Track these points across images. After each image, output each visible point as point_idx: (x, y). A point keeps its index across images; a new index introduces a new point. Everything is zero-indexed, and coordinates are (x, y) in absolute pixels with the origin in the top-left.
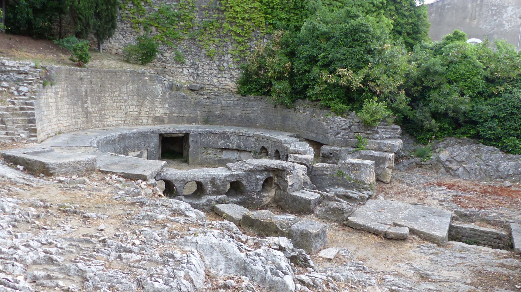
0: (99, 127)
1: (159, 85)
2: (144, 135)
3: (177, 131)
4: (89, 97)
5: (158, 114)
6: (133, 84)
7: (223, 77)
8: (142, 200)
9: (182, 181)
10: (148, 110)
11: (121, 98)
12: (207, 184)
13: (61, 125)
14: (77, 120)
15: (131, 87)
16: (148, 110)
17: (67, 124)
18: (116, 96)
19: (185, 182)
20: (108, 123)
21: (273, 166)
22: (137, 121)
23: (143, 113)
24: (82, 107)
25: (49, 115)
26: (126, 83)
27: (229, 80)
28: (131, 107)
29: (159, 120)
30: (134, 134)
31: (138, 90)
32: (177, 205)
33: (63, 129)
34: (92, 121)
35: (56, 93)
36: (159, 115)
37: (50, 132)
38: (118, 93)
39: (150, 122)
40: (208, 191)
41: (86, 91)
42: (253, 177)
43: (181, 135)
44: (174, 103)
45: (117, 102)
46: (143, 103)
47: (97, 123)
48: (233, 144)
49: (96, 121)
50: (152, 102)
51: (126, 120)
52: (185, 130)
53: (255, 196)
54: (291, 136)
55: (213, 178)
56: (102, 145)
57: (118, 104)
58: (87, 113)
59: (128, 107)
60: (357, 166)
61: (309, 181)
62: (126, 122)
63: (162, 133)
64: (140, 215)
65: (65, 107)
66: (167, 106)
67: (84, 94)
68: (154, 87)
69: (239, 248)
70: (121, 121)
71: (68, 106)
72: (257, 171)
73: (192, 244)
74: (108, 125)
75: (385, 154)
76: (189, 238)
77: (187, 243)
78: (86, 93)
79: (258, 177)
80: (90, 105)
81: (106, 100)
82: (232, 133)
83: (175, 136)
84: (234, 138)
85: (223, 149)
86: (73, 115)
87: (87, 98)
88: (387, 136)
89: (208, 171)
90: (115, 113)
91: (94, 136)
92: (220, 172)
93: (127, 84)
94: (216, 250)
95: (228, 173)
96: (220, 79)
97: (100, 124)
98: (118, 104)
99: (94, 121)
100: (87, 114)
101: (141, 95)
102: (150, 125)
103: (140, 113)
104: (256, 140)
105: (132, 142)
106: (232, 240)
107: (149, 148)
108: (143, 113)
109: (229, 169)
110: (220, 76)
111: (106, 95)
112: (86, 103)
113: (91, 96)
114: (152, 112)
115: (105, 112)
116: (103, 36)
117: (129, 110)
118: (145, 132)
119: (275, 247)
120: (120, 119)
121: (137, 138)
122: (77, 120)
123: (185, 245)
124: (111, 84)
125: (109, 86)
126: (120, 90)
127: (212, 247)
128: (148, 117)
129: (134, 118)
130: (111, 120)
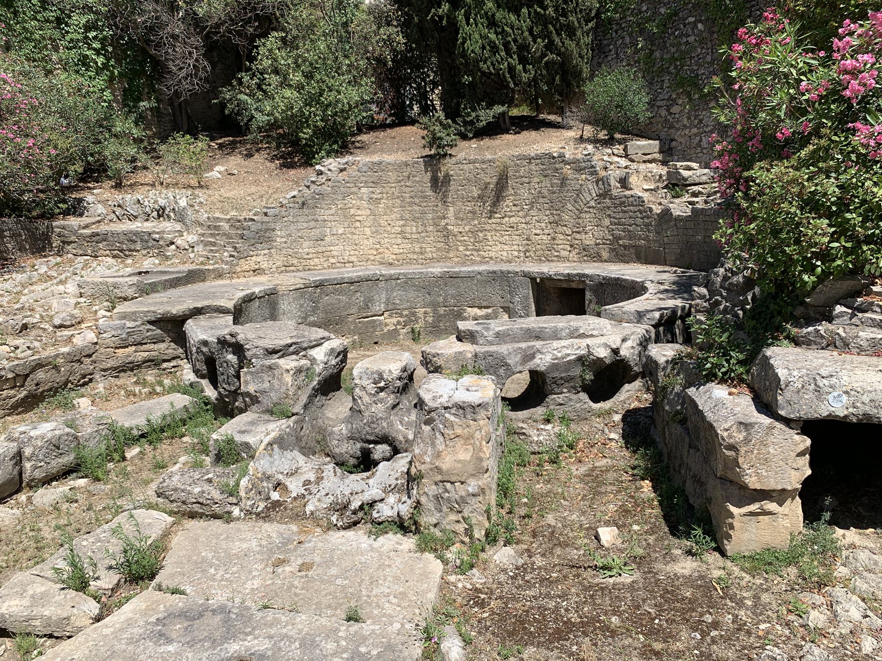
10: (569, 232)
11: (519, 208)
14: (424, 245)
18: (507, 206)
20: (492, 254)
30: (480, 273)
37: (353, 259)
43: (574, 285)
45: (510, 217)
47: (468, 253)
51: (527, 251)
52: (578, 275)
57: (513, 219)
58: (447, 235)
62: (528, 254)
65: (393, 221)
66: (607, 222)
71: (402, 222)
74: (491, 258)
83: (565, 286)
90: (507, 237)
99: (461, 248)
103: (554, 239)
112: (444, 218)
114: (578, 236)
122: (424, 245)
128: (571, 246)
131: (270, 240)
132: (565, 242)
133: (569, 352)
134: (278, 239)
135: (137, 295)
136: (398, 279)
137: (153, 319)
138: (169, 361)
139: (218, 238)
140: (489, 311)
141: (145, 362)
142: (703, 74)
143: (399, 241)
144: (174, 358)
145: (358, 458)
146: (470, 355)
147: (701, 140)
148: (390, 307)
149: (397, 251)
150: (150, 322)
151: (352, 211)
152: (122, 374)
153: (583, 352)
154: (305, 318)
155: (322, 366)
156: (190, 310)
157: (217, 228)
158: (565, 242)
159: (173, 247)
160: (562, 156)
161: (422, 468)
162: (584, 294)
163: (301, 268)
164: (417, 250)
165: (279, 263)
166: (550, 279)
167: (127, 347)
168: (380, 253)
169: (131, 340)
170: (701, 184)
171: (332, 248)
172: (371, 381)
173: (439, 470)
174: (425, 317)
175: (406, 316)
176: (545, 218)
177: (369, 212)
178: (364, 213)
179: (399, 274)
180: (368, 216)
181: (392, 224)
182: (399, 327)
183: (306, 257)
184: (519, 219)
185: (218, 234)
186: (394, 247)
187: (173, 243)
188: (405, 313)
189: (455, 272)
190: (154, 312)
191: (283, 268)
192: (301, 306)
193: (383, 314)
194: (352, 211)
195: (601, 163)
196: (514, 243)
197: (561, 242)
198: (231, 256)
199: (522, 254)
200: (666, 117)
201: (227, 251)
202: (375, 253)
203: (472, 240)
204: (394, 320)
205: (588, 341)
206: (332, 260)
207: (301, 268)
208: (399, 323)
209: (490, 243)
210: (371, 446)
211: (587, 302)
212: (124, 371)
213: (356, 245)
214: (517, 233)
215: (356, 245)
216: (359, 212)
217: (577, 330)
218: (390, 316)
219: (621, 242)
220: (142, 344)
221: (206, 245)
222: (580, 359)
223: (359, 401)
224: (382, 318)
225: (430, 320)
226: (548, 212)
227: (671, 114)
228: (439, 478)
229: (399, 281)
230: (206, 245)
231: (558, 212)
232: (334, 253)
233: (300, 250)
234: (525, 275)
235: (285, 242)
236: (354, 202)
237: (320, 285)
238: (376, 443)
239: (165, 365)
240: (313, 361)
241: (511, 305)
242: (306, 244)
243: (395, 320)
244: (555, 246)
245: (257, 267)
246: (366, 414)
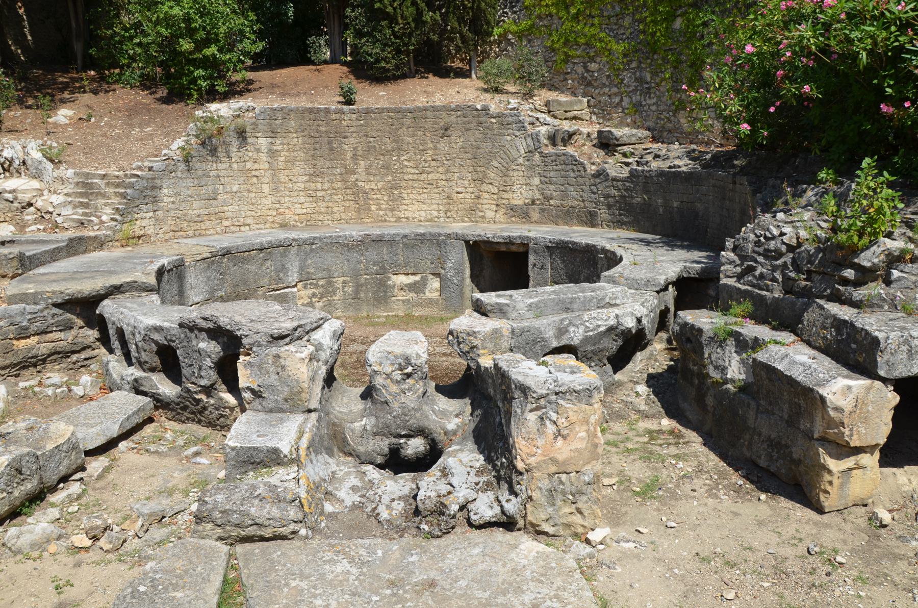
0: (385, 221)
3: (503, 238)
10: (495, 190)
11: (438, 163)
13: (287, 211)
14: (330, 204)
16: (495, 190)
17: (305, 211)
18: (425, 161)
20: (408, 214)
22: (472, 211)
25: (249, 191)
29: (521, 213)
30: (406, 236)
33: (290, 217)
35: (272, 153)
36: (520, 202)
37: (249, 221)
38: (430, 152)
43: (514, 248)
44: (552, 174)
46: (485, 176)
47: (381, 213)
51: (449, 210)
52: (519, 237)
55: (135, 327)
57: (430, 176)
58: (357, 192)
59: (453, 183)
62: (449, 214)
66: (536, 181)
67: (349, 156)
68: (509, 138)
70: (439, 211)
71: (306, 178)
72: (201, 330)
74: (407, 218)
79: (202, 345)
83: (503, 249)
86: (320, 194)
97: (390, 214)
99: (373, 208)
102: (501, 222)
103: (478, 197)
108: (486, 195)
114: (506, 195)
120: (435, 206)
122: (330, 204)
126: (435, 148)
128: (497, 205)
129: (467, 207)
130: (415, 207)
131: (155, 200)
132: (490, 202)
133: (599, 323)
134: (165, 199)
135: (20, 271)
136: (313, 244)
137: (60, 301)
138: (78, 352)
139: (91, 198)
140: (417, 278)
141: (49, 356)
142: (623, 34)
143: (302, 200)
144: (84, 349)
145: (386, 455)
146: (506, 333)
147: (621, 100)
148: (305, 277)
149: (299, 211)
150: (56, 305)
151: (249, 165)
152: (23, 373)
153: (612, 323)
154: (211, 293)
155: (328, 352)
156: (107, 288)
157: (90, 186)
158: (490, 202)
159: (32, 209)
160: (485, 109)
161: (532, 461)
162: (528, 258)
163: (191, 233)
164: (323, 210)
165: (165, 228)
166: (488, 243)
167: (29, 337)
168: (280, 214)
169: (34, 328)
170: (630, 144)
171: (226, 208)
172: (397, 366)
173: (553, 460)
174: (344, 287)
175: (322, 286)
176: (468, 175)
177: (267, 166)
178: (262, 167)
179: (315, 238)
180: (266, 170)
181: (294, 179)
182: (314, 300)
183: (197, 219)
184: (438, 175)
185: (92, 194)
186: (297, 207)
187: (30, 205)
188: (321, 283)
189: (378, 236)
190: (61, 292)
191: (171, 234)
192: (209, 278)
193: (296, 285)
194: (249, 165)
195: (528, 119)
197: (485, 201)
198: (112, 219)
199: (442, 214)
200: (583, 74)
201: (106, 213)
202: (274, 214)
203: (385, 198)
204: (309, 292)
205: (616, 311)
206: (226, 223)
207: (191, 233)
208: (314, 295)
210: (402, 441)
211: (530, 267)
212: (24, 367)
213: (253, 204)
214: (437, 191)
215: (253, 204)
216: (256, 166)
217: (603, 299)
218: (305, 287)
219: (552, 202)
220: (46, 333)
221: (75, 207)
222: (611, 329)
223: (384, 391)
224: (295, 289)
225: (349, 290)
226: (471, 169)
227: (588, 71)
228: (554, 469)
229: (314, 247)
230: (75, 207)
231: (482, 169)
232: (228, 214)
233: (190, 212)
234: (457, 237)
235: (173, 202)
236: (250, 154)
237: (227, 253)
238: (408, 436)
239: (75, 357)
240: (319, 347)
241: (442, 271)
242: (196, 204)
243: (309, 292)
244: (480, 206)
245: (142, 233)
246: (396, 405)
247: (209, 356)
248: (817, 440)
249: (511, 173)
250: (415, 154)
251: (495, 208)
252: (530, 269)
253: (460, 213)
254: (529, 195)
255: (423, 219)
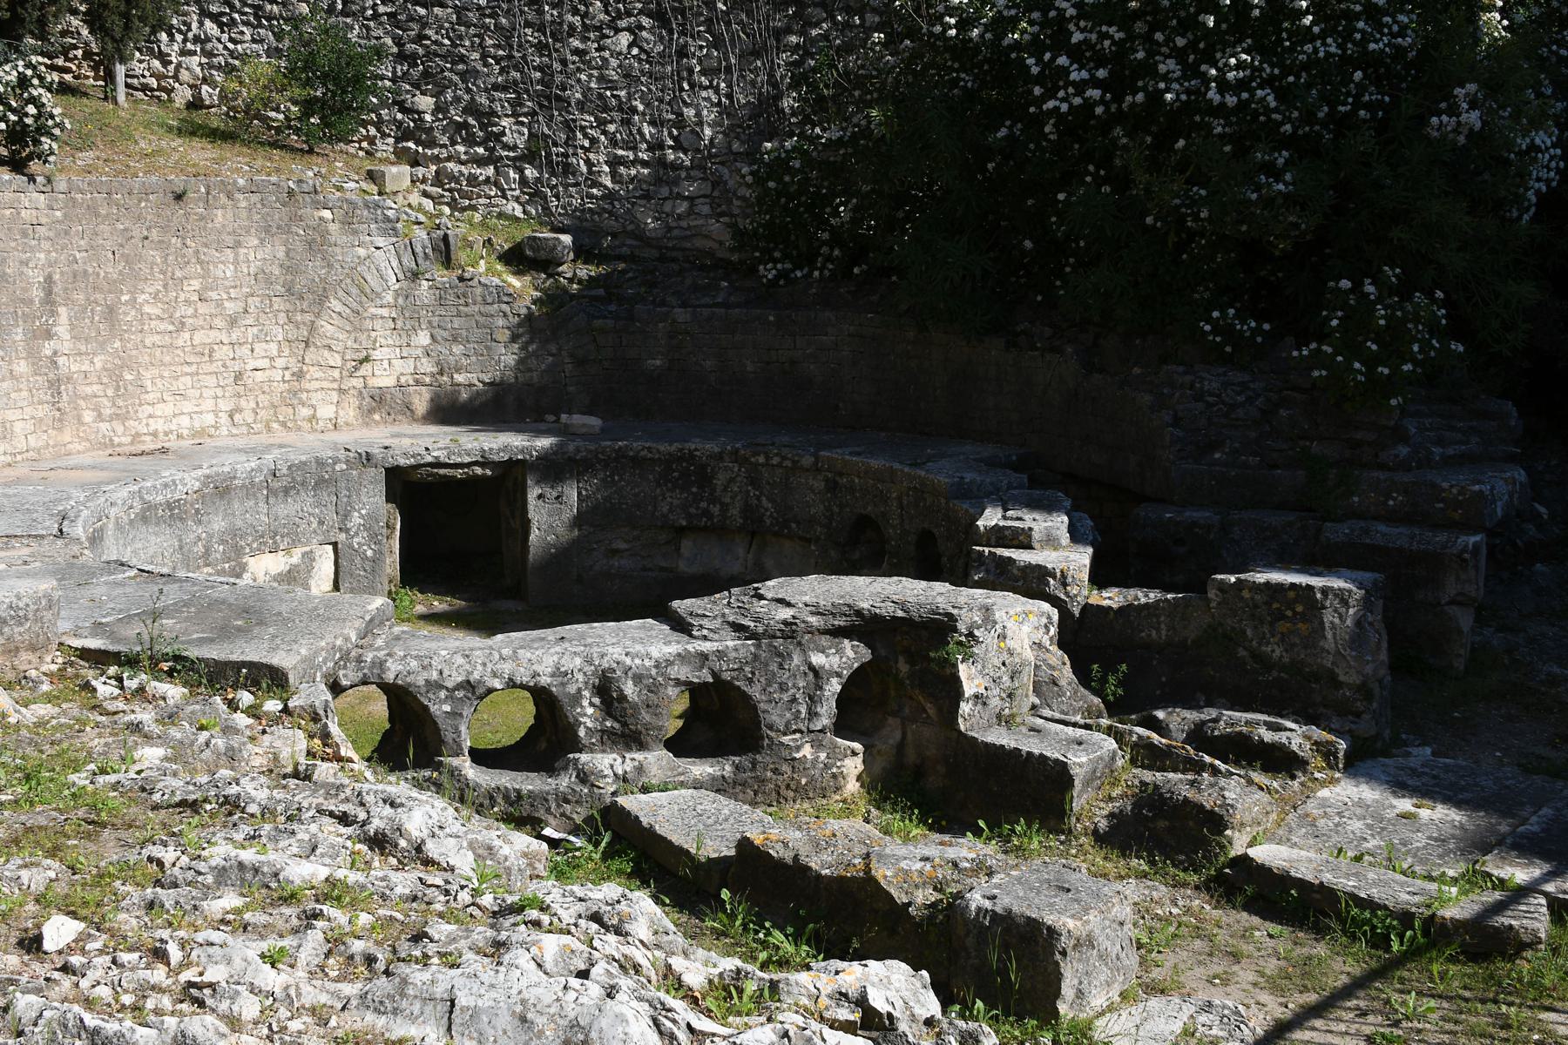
1: (380, 241)
2: (314, 478)
4: (62, 310)
5: (384, 379)
6: (262, 241)
7: (680, 196)
8: (233, 790)
9: (459, 687)
12: (576, 699)
15: (258, 254)
16: (336, 360)
19: (473, 690)
20: (158, 425)
21: (887, 610)
23: (314, 372)
24: (33, 355)
26: (229, 240)
27: (706, 209)
28: (259, 347)
31: (290, 269)
32: (388, 811)
34: (79, 418)
36: (388, 382)
38: (196, 284)
39: (349, 413)
40: (582, 733)
41: (49, 279)
42: (797, 660)
46: (312, 328)
47: (104, 426)
48: (725, 508)
49: (100, 417)
50: (356, 321)
51: (239, 410)
53: (807, 751)
54: (991, 463)
56: (119, 527)
57: (199, 337)
59: (245, 350)
60: (1296, 601)
61: (1066, 674)
63: (402, 462)
64: (202, 867)
66: (423, 338)
67: (37, 294)
68: (362, 252)
69: (657, 1024)
70: (216, 413)
73: (429, 1008)
75: (1442, 537)
76: (418, 976)
77: (404, 1003)
78: (49, 293)
80: (66, 346)
81: (143, 317)
82: (720, 457)
84: (732, 480)
85: (681, 531)
87: (53, 313)
88: (1450, 451)
89: (582, 636)
91: (83, 486)
92: (636, 646)
93: (238, 244)
94: (541, 1032)
95: (673, 649)
96: (667, 207)
97: (120, 429)
98: (199, 337)
99: (88, 416)
100: (55, 385)
101: (303, 293)
103: (299, 375)
104: (832, 486)
105: (263, 507)
106: (625, 983)
107: (343, 536)
108: (314, 372)
109: (681, 626)
110: (665, 191)
111: (141, 298)
112: (49, 335)
113: (68, 301)
115: (139, 376)
116: (127, 27)
117: (252, 364)
118: (320, 463)
119: (845, 1014)
121: (286, 491)
123: (395, 1012)
124: (162, 245)
125: (155, 255)
126: (206, 275)
127: (523, 1019)
128: (341, 391)
130: (168, 409)
132: (325, 384)
158: (325, 384)
184: (213, 333)
196: (208, 393)
197: (316, 385)
199: (224, 418)
209: (150, 397)
244: (304, 396)
247: (839, 675)
248: (1451, 603)
249: (368, 324)
250: (165, 286)
251: (335, 396)
252: (531, 508)
253: (262, 413)
254: (409, 366)
255: (185, 432)
